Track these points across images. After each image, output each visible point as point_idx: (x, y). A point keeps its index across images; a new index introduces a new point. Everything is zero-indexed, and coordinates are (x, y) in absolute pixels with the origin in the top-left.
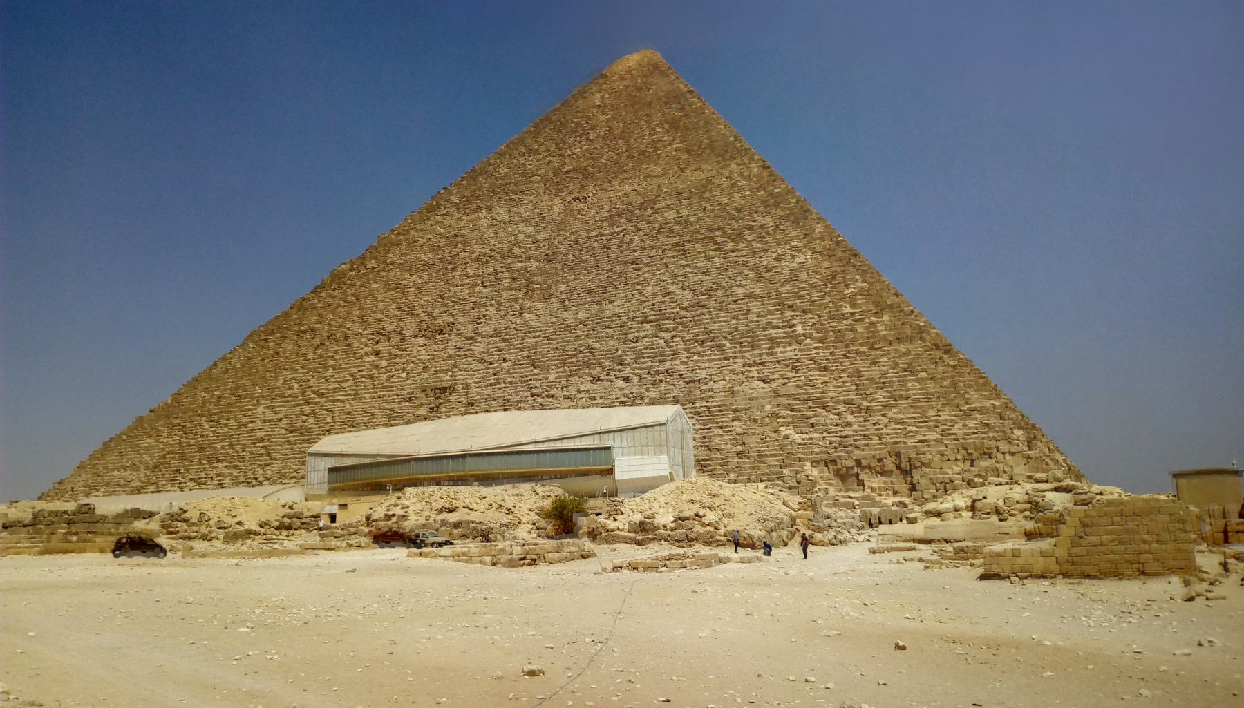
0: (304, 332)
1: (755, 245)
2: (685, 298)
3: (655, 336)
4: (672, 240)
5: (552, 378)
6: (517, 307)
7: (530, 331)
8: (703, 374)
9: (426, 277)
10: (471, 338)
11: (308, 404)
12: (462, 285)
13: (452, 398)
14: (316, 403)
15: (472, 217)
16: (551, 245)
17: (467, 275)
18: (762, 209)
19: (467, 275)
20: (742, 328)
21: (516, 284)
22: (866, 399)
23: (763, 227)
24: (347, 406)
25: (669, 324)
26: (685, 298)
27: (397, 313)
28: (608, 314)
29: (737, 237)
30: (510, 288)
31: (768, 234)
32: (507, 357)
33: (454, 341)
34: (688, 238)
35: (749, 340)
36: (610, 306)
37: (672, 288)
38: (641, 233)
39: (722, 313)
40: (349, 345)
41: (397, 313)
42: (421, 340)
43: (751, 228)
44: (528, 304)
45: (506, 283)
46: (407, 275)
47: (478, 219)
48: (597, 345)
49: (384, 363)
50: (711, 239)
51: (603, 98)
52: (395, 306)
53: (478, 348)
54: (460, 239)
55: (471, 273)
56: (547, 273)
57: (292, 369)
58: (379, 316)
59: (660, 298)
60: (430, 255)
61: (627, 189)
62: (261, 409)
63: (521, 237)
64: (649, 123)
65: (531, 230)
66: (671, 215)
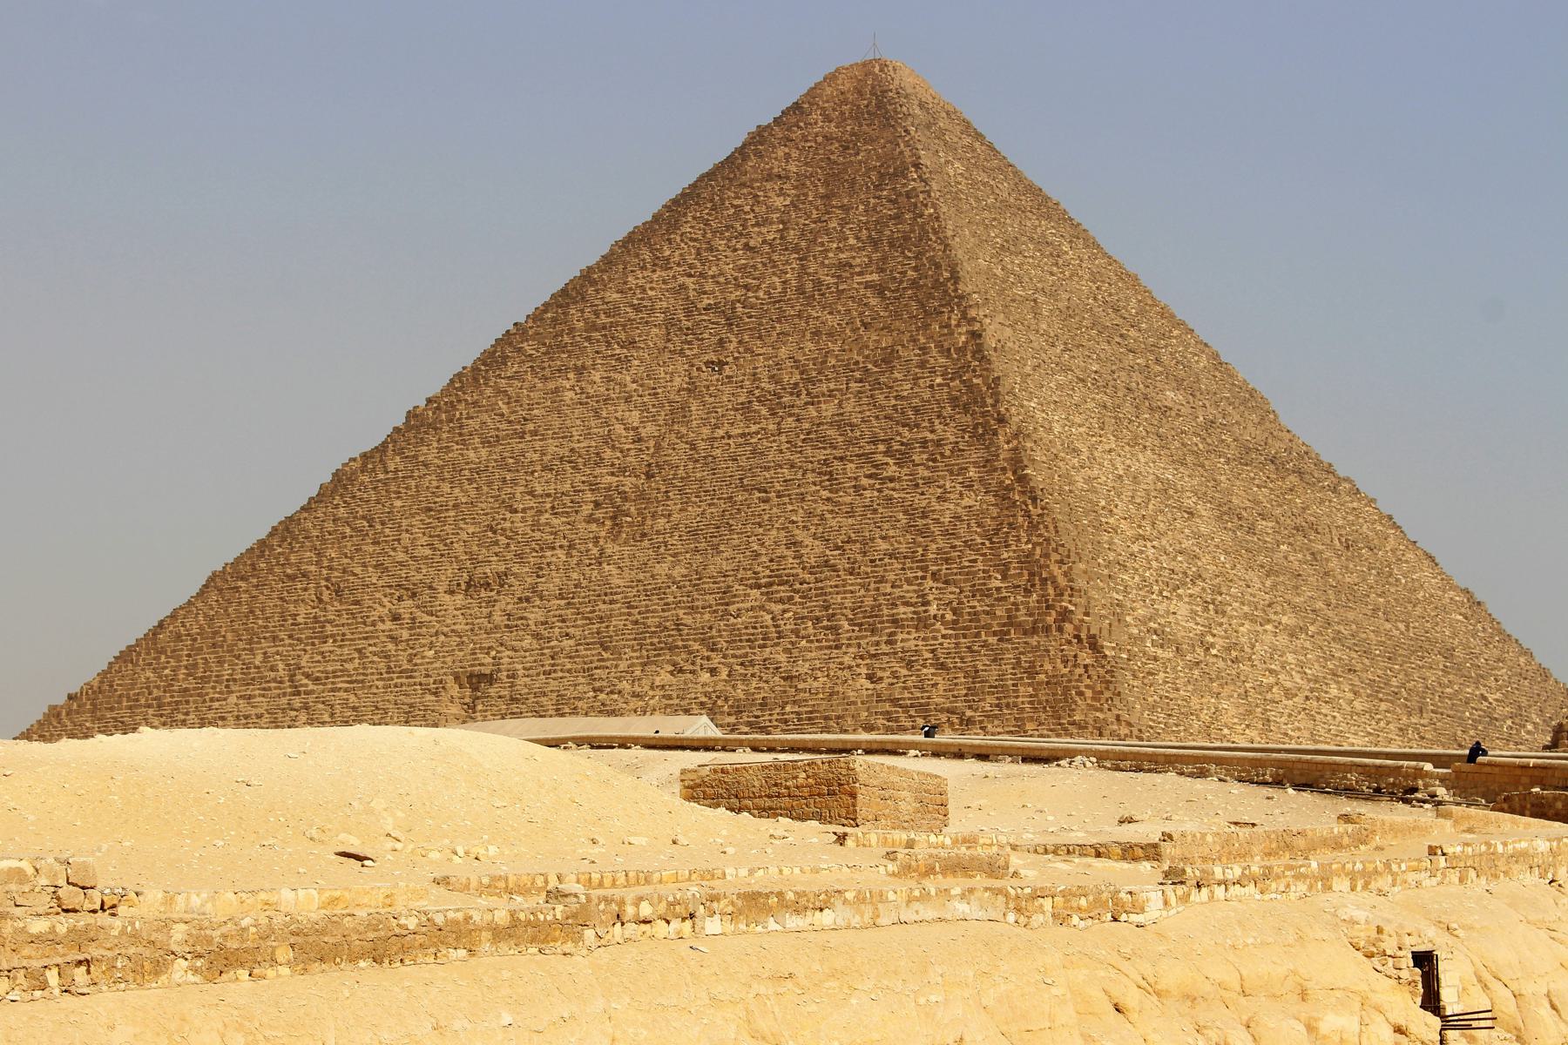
0: (292, 578)
1: (923, 472)
2: (814, 550)
3: (762, 608)
4: (821, 455)
5: (623, 665)
6: (595, 551)
7: (608, 595)
8: (803, 668)
9: (473, 493)
10: (528, 600)
11: (298, 693)
12: (524, 511)
13: (492, 691)
14: (312, 692)
15: (551, 385)
16: (658, 447)
17: (531, 493)
18: (948, 411)
19: (531, 493)
21: (599, 514)
22: (970, 707)
23: (938, 443)
24: (352, 698)
25: (782, 591)
26: (814, 550)
27: (428, 552)
28: (712, 570)
29: (903, 459)
30: (590, 519)
31: (942, 455)
32: (571, 631)
33: (505, 603)
34: (838, 453)
35: (868, 621)
37: (800, 535)
38: (783, 438)
39: (851, 579)
40: (357, 603)
41: (428, 552)
42: (459, 599)
43: (924, 443)
44: (610, 548)
45: (587, 509)
46: (446, 487)
48: (688, 620)
49: (405, 634)
50: (866, 457)
51: (787, 156)
52: (424, 540)
53: (534, 615)
54: (531, 426)
55: (539, 490)
56: (642, 496)
57: (274, 638)
58: (401, 556)
60: (484, 452)
62: (233, 699)
64: (844, 222)
65: (634, 417)
66: (829, 409)
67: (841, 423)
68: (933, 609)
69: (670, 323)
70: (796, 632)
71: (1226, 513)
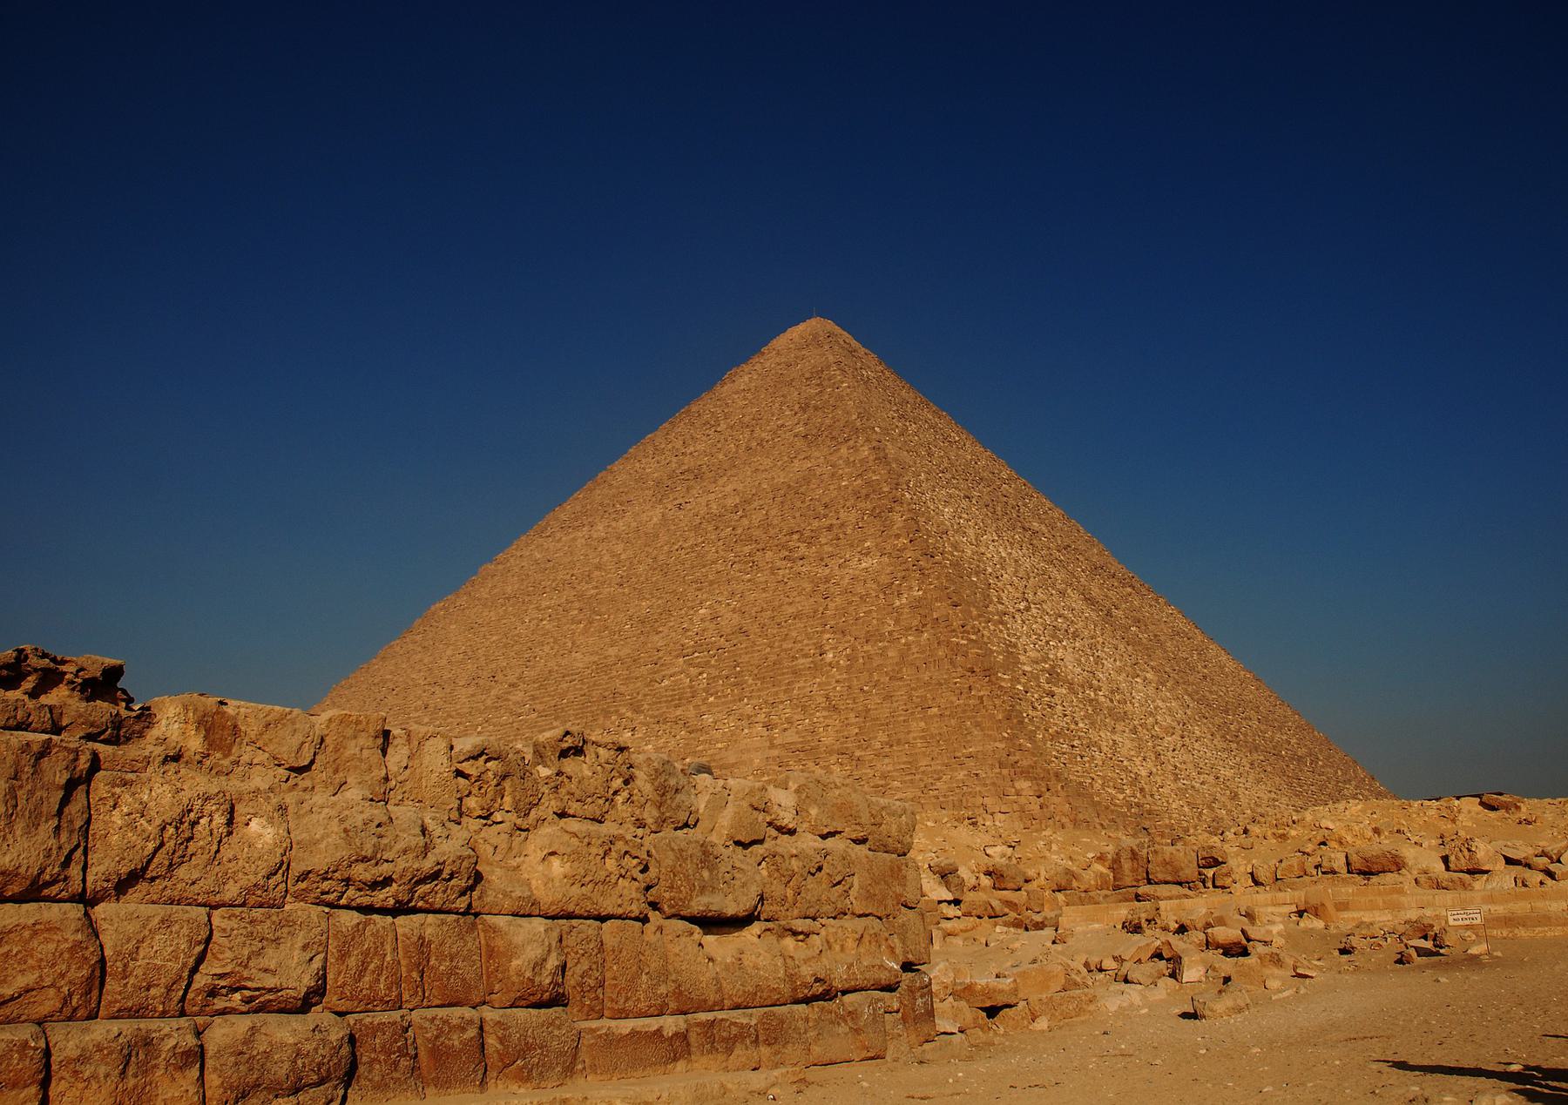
4: (747, 549)
20: (773, 658)
36: (656, 638)
42: (471, 690)
47: (574, 539)
48: (622, 689)
61: (729, 488)
66: (757, 518)
69: (658, 483)
70: (706, 690)
71: (1090, 601)
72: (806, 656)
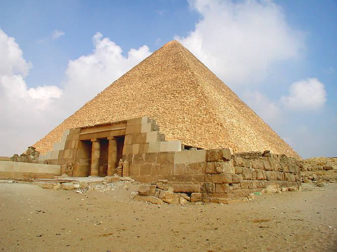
26: (162, 110)
30: (123, 108)
37: (159, 107)
50: (172, 94)
58: (92, 116)
59: (156, 110)
63: (129, 93)
66: (165, 87)
67: (167, 88)
68: (186, 119)
72: (180, 119)
